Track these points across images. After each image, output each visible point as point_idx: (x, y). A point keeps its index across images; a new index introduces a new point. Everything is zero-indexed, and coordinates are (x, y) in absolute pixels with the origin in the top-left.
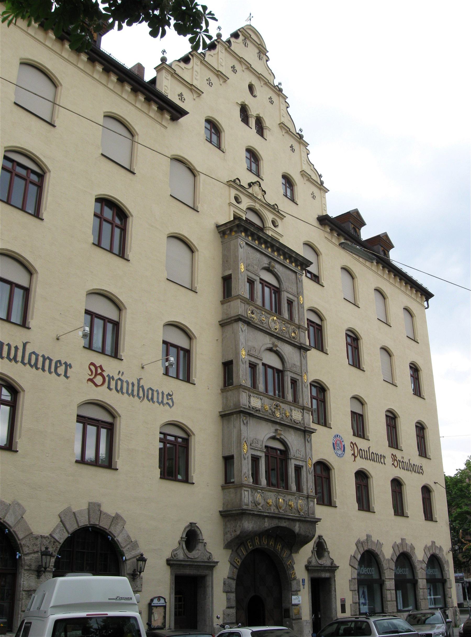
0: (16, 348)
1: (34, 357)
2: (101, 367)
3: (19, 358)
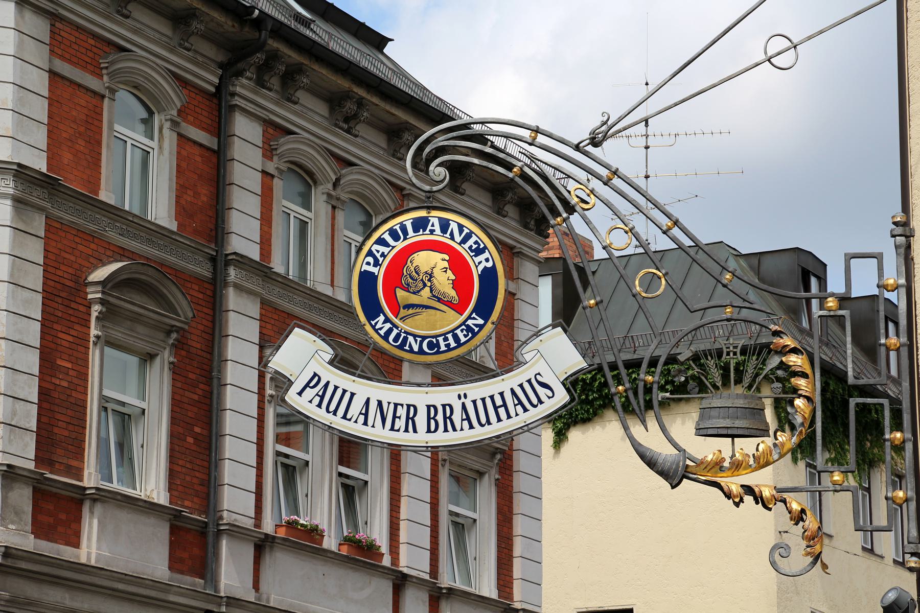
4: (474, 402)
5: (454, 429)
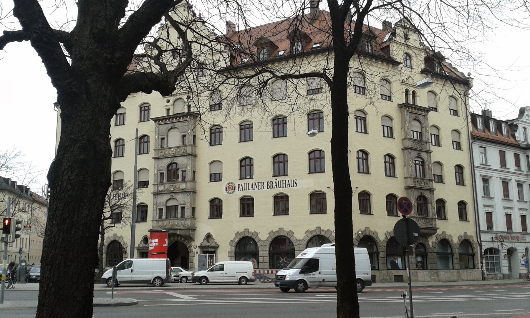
4: (279, 181)
5: (273, 188)
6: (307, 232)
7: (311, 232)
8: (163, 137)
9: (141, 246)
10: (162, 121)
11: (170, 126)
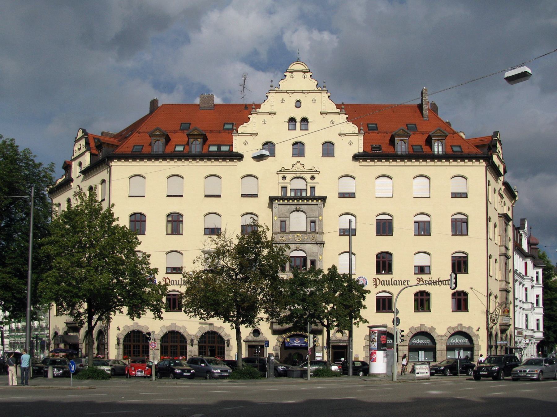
0: (389, 281)
1: (395, 282)
2: (422, 278)
3: (390, 284)
6: (449, 328)
7: (453, 328)
8: (284, 219)
9: (250, 338)
10: (288, 201)
11: (294, 208)
